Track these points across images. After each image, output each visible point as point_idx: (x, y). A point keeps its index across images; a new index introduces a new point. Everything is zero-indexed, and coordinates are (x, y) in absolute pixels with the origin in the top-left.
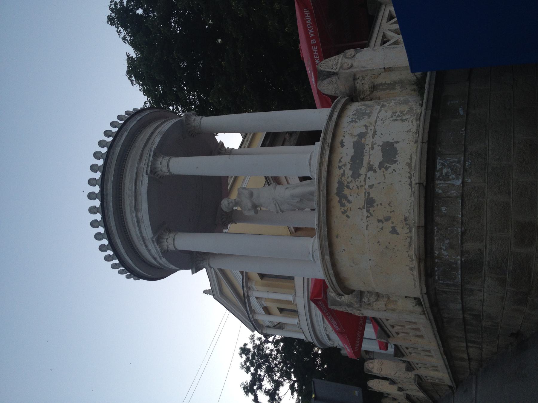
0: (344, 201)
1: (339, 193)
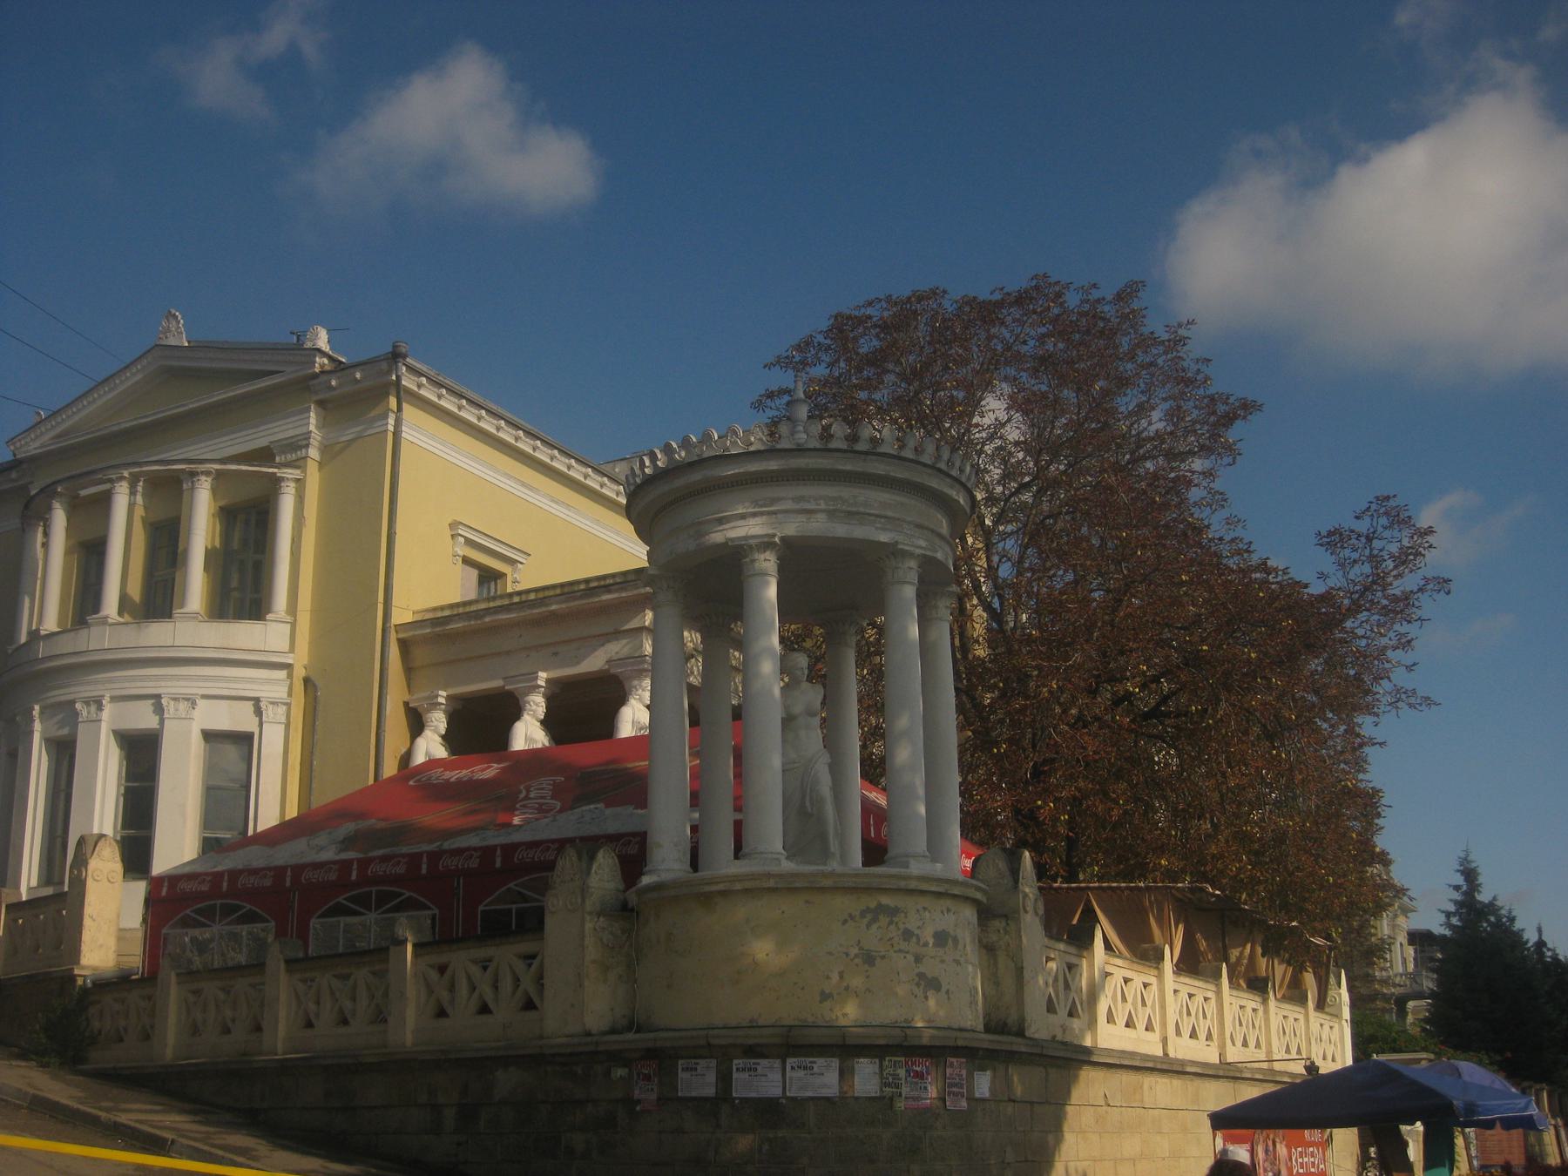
0: (869, 917)
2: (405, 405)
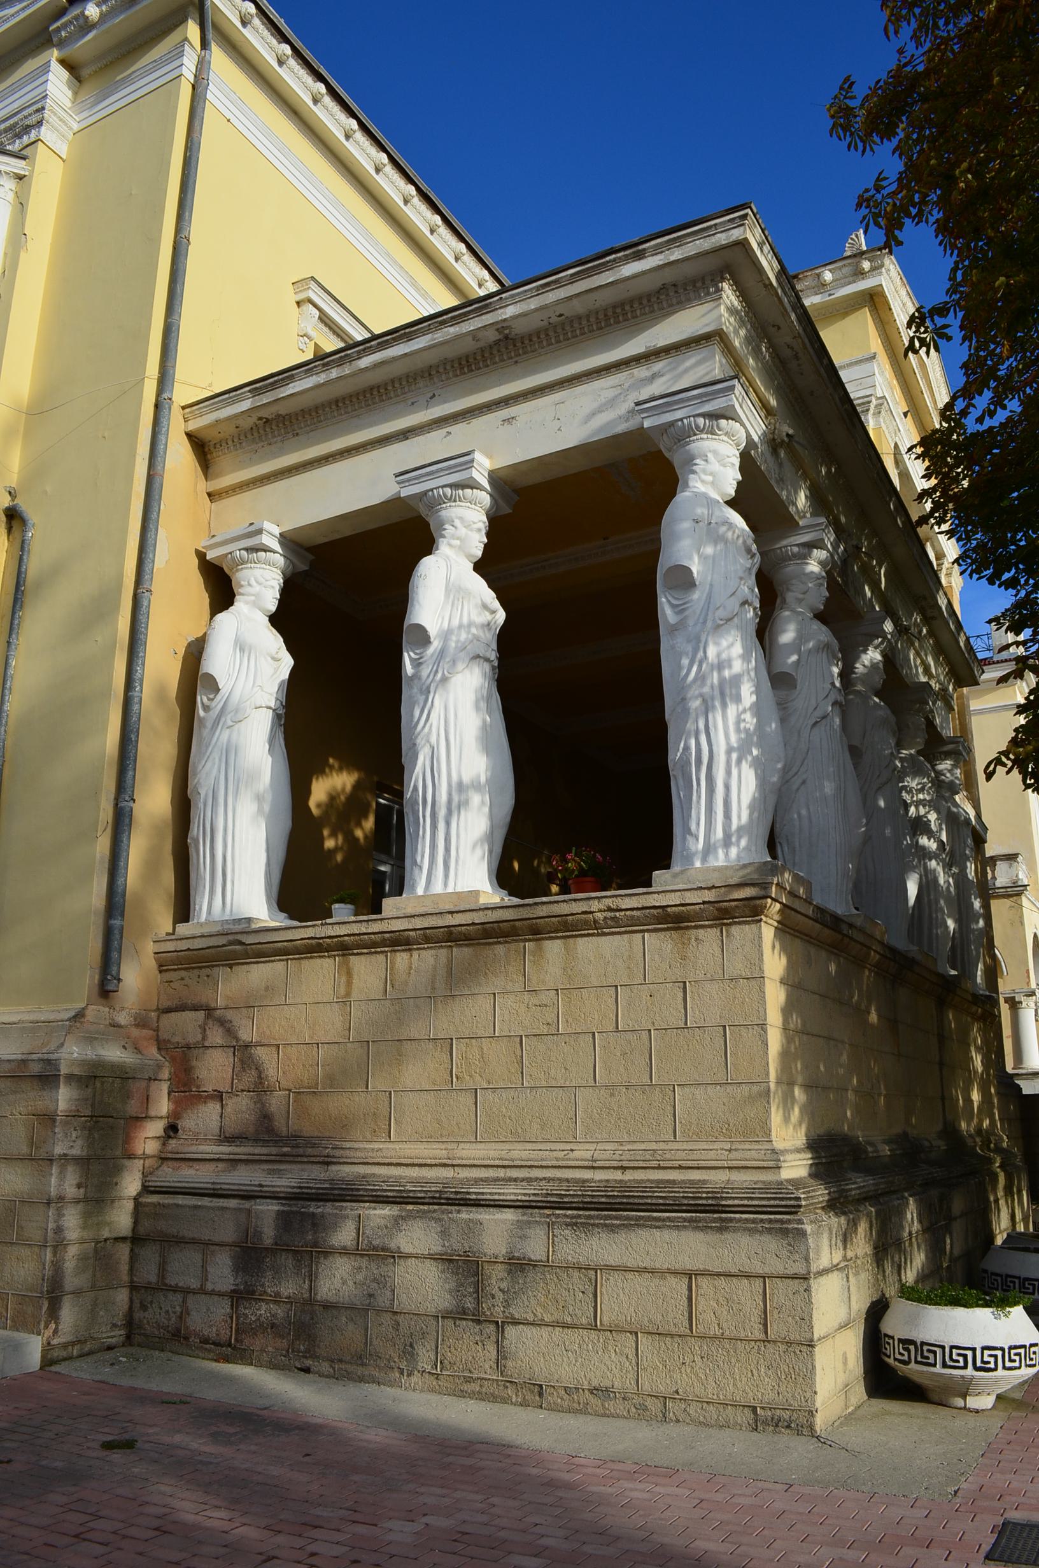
2: (214, 48)
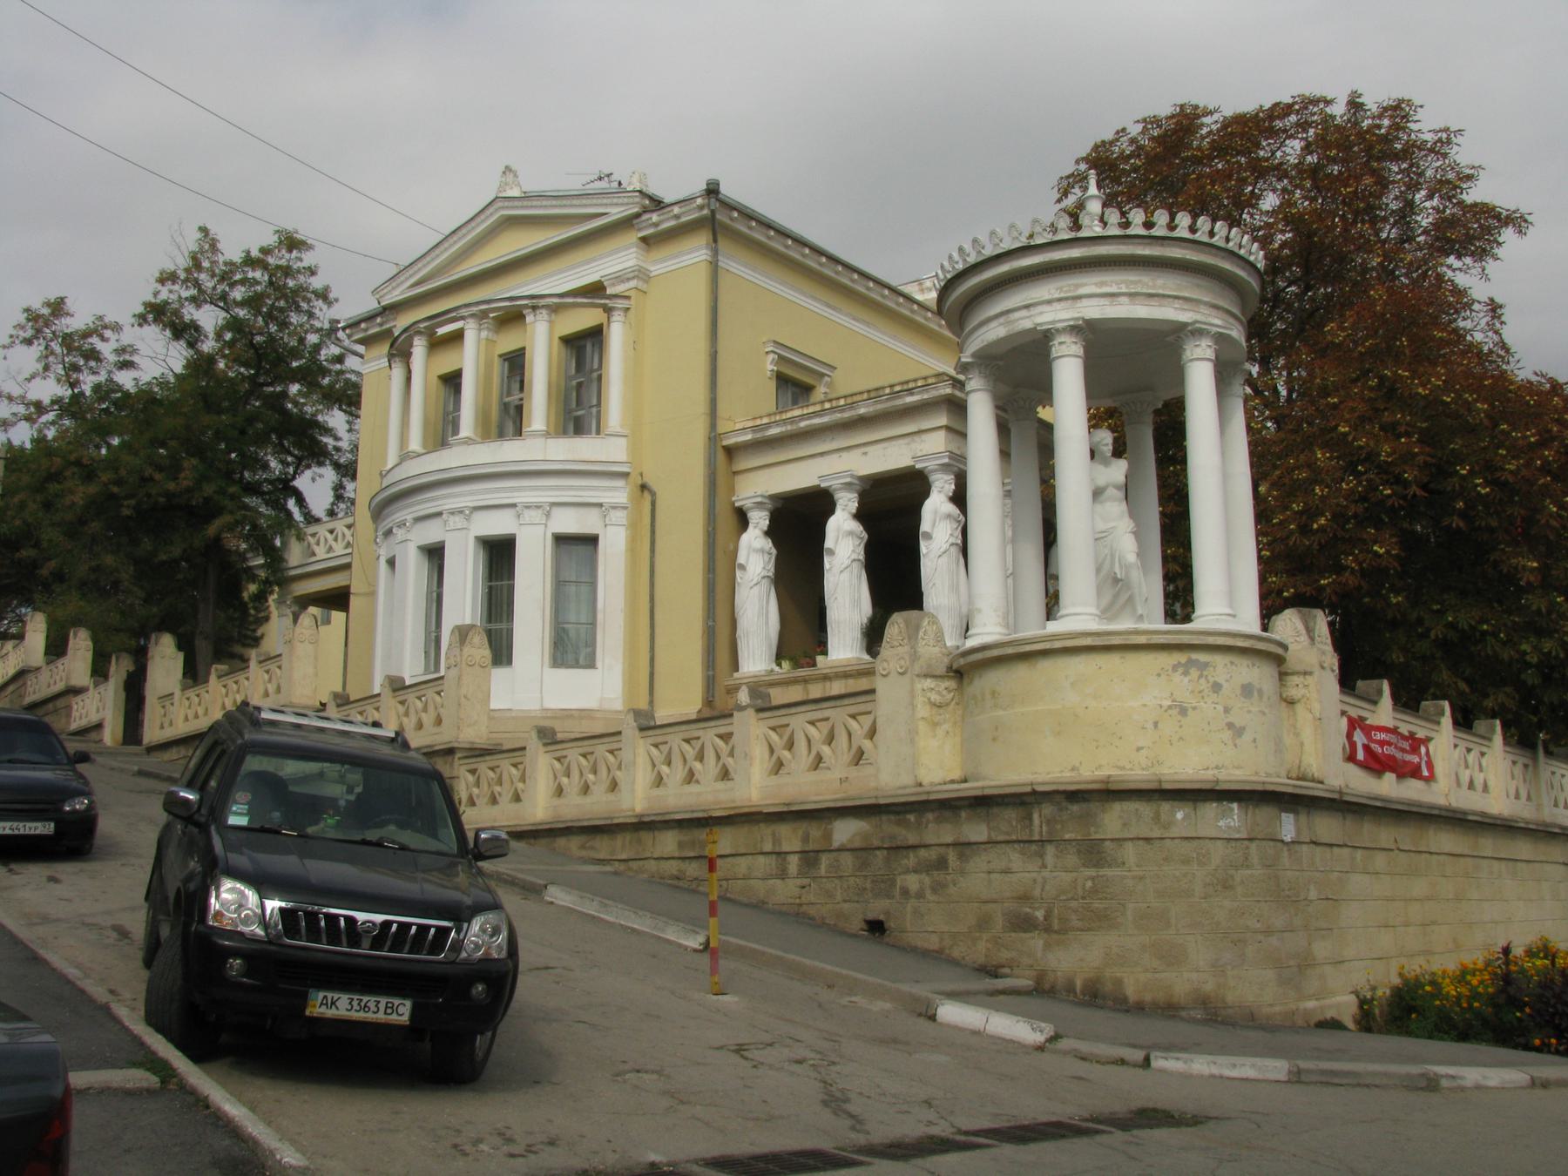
0: (1181, 670)
1: (1190, 662)
